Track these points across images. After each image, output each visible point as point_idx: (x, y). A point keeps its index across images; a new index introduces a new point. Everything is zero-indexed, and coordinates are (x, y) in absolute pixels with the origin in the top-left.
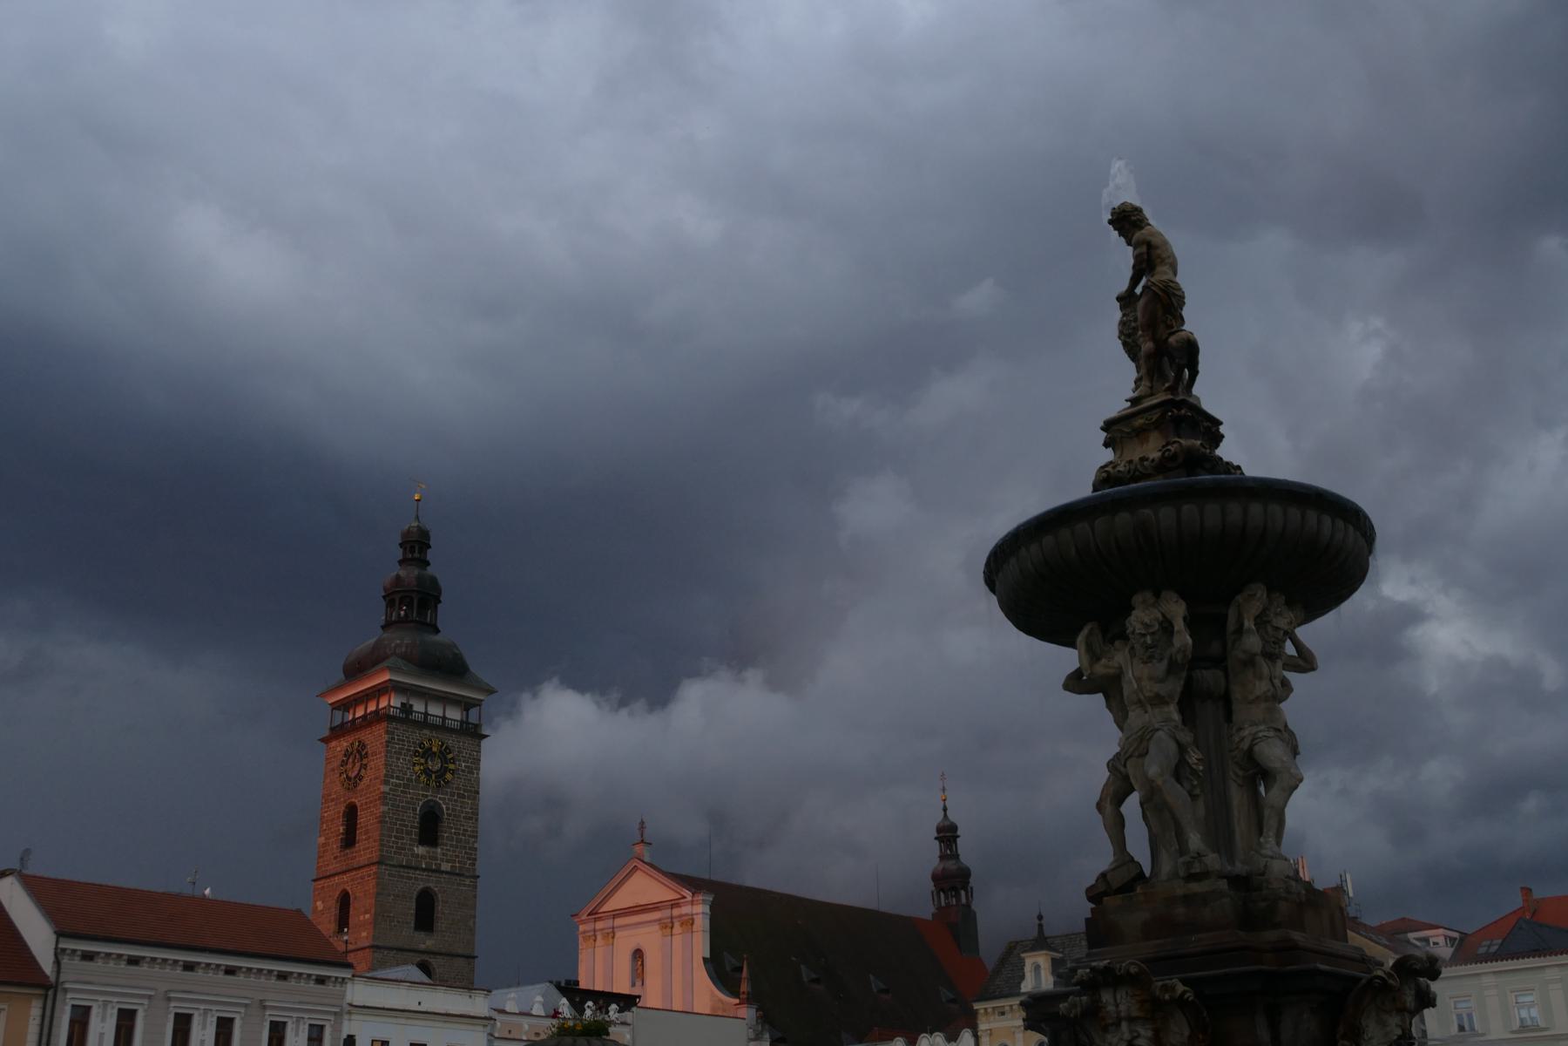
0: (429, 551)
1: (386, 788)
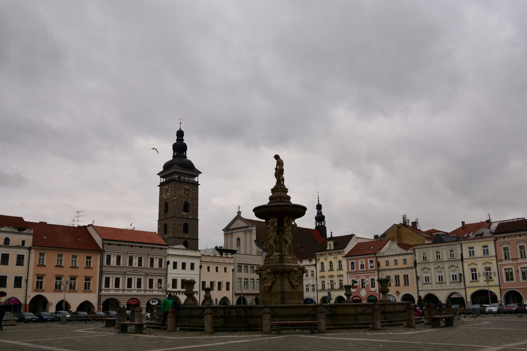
1: (175, 198)
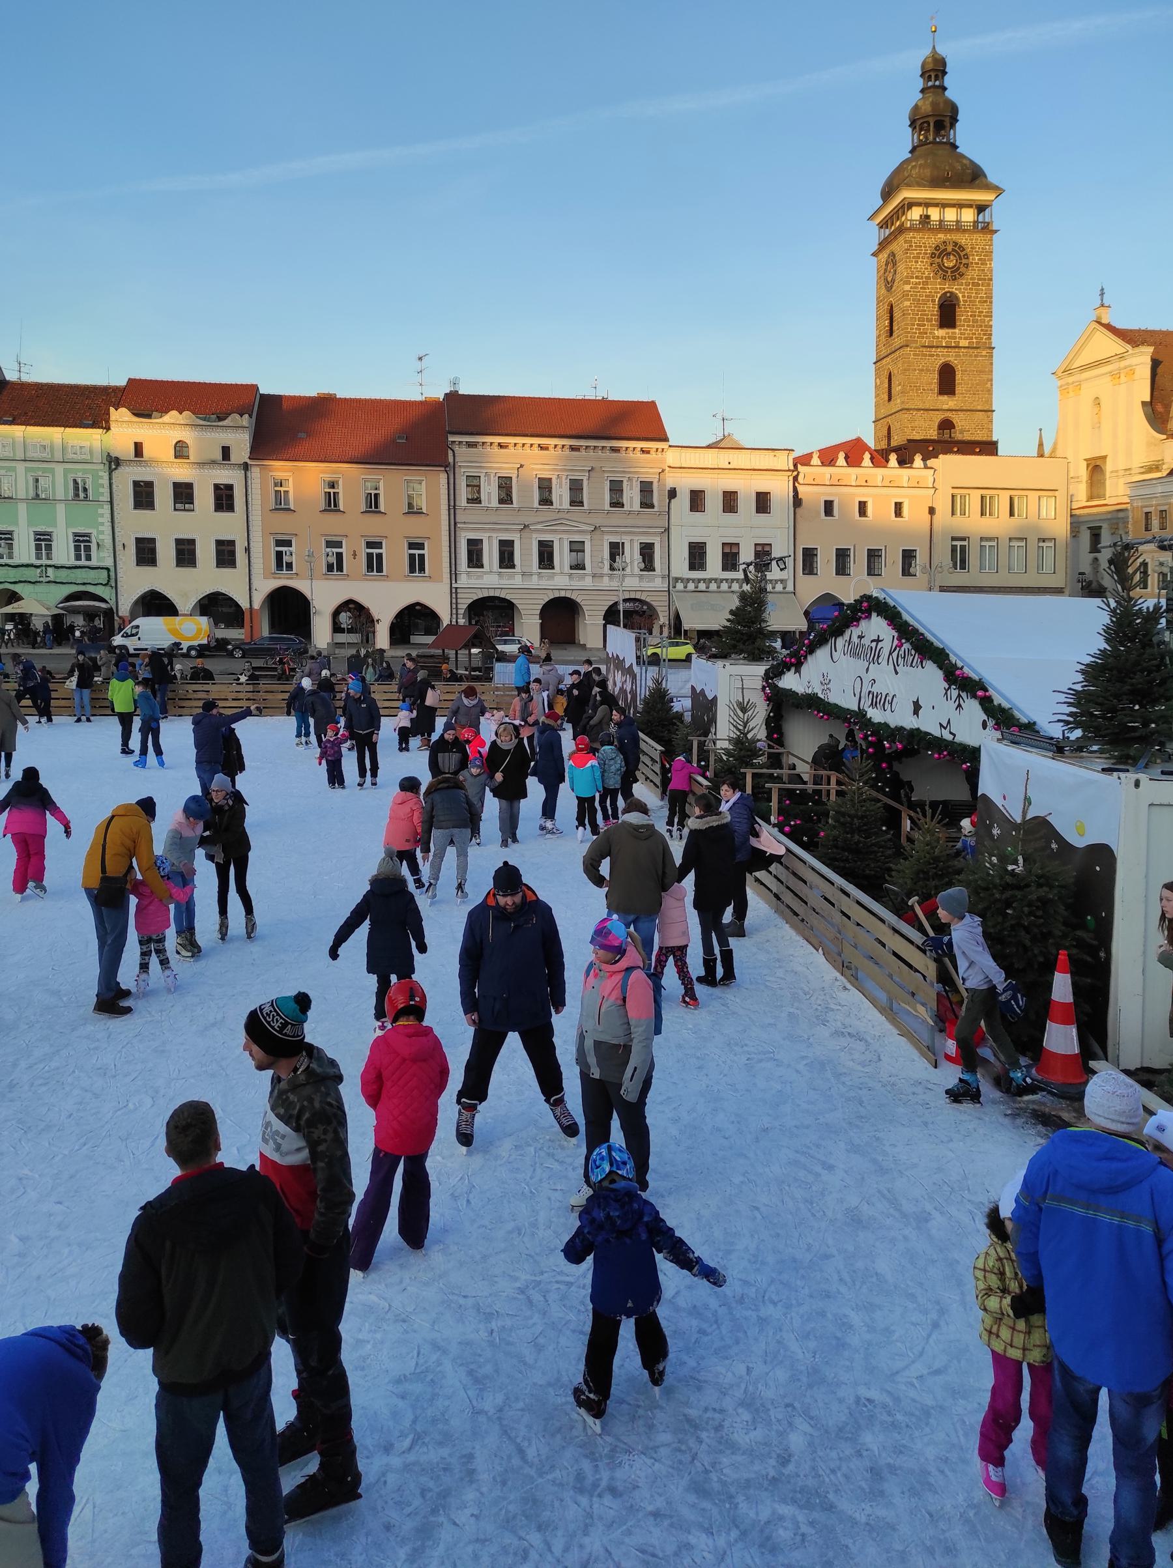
0: (946, 77)
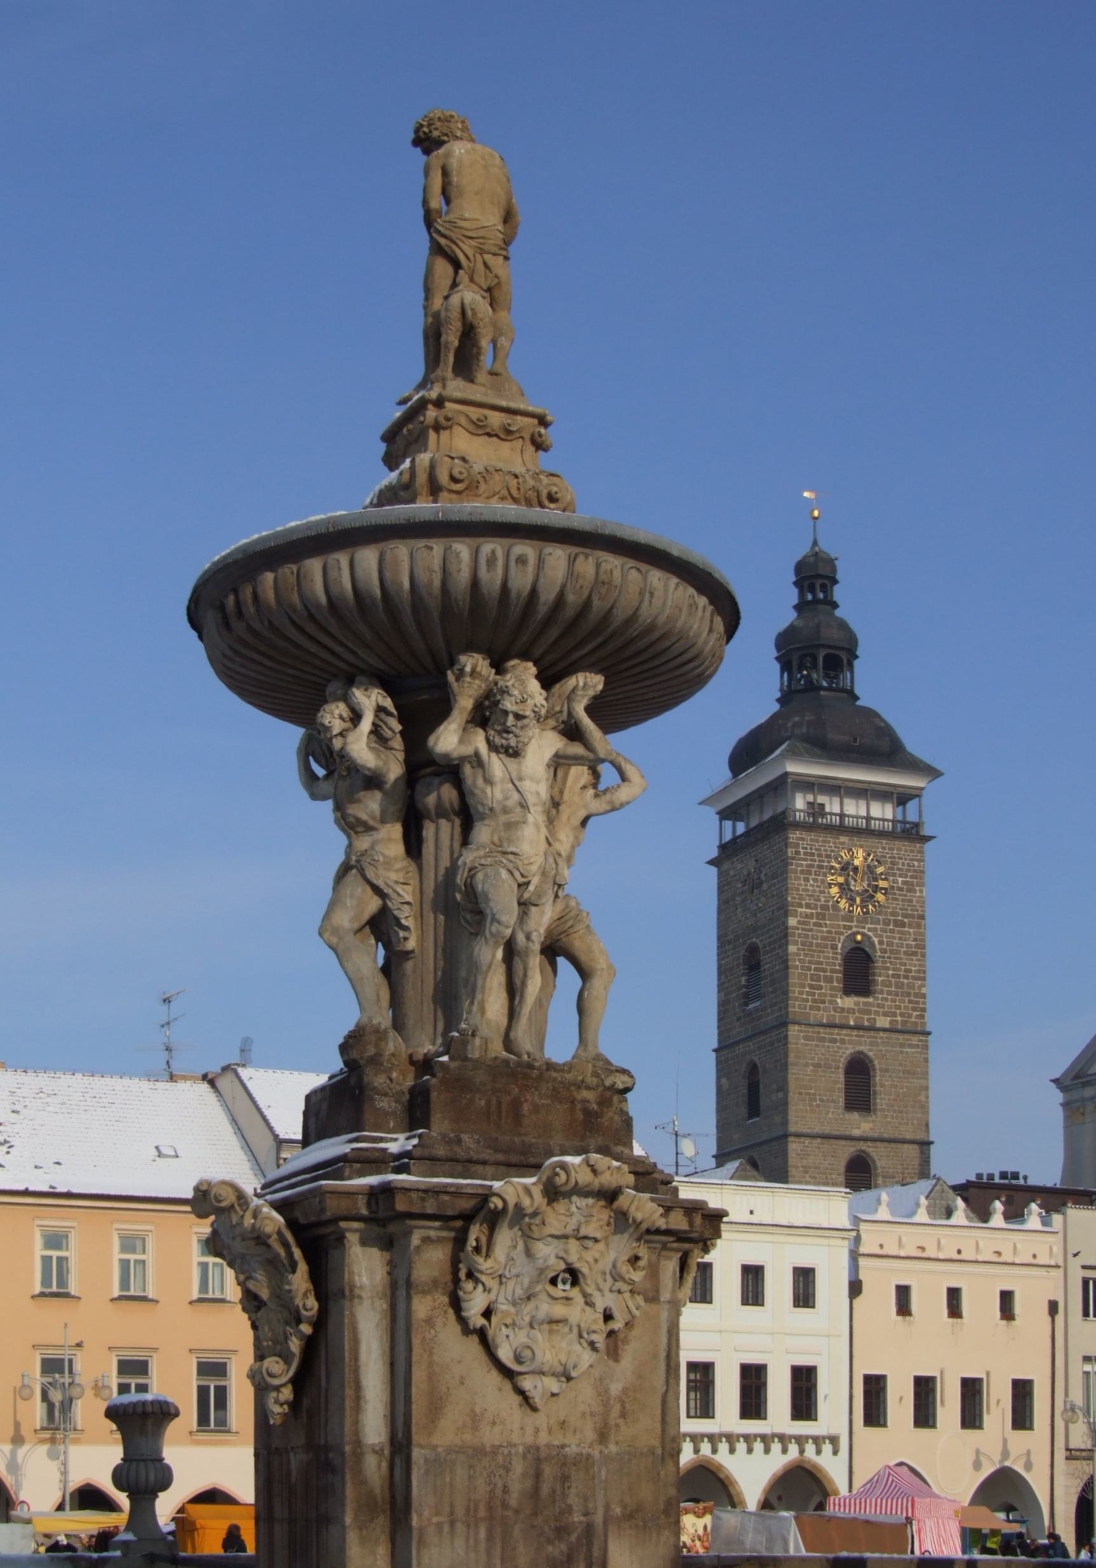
0: (836, 588)
